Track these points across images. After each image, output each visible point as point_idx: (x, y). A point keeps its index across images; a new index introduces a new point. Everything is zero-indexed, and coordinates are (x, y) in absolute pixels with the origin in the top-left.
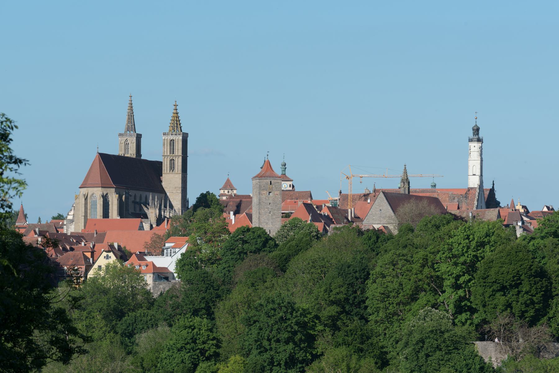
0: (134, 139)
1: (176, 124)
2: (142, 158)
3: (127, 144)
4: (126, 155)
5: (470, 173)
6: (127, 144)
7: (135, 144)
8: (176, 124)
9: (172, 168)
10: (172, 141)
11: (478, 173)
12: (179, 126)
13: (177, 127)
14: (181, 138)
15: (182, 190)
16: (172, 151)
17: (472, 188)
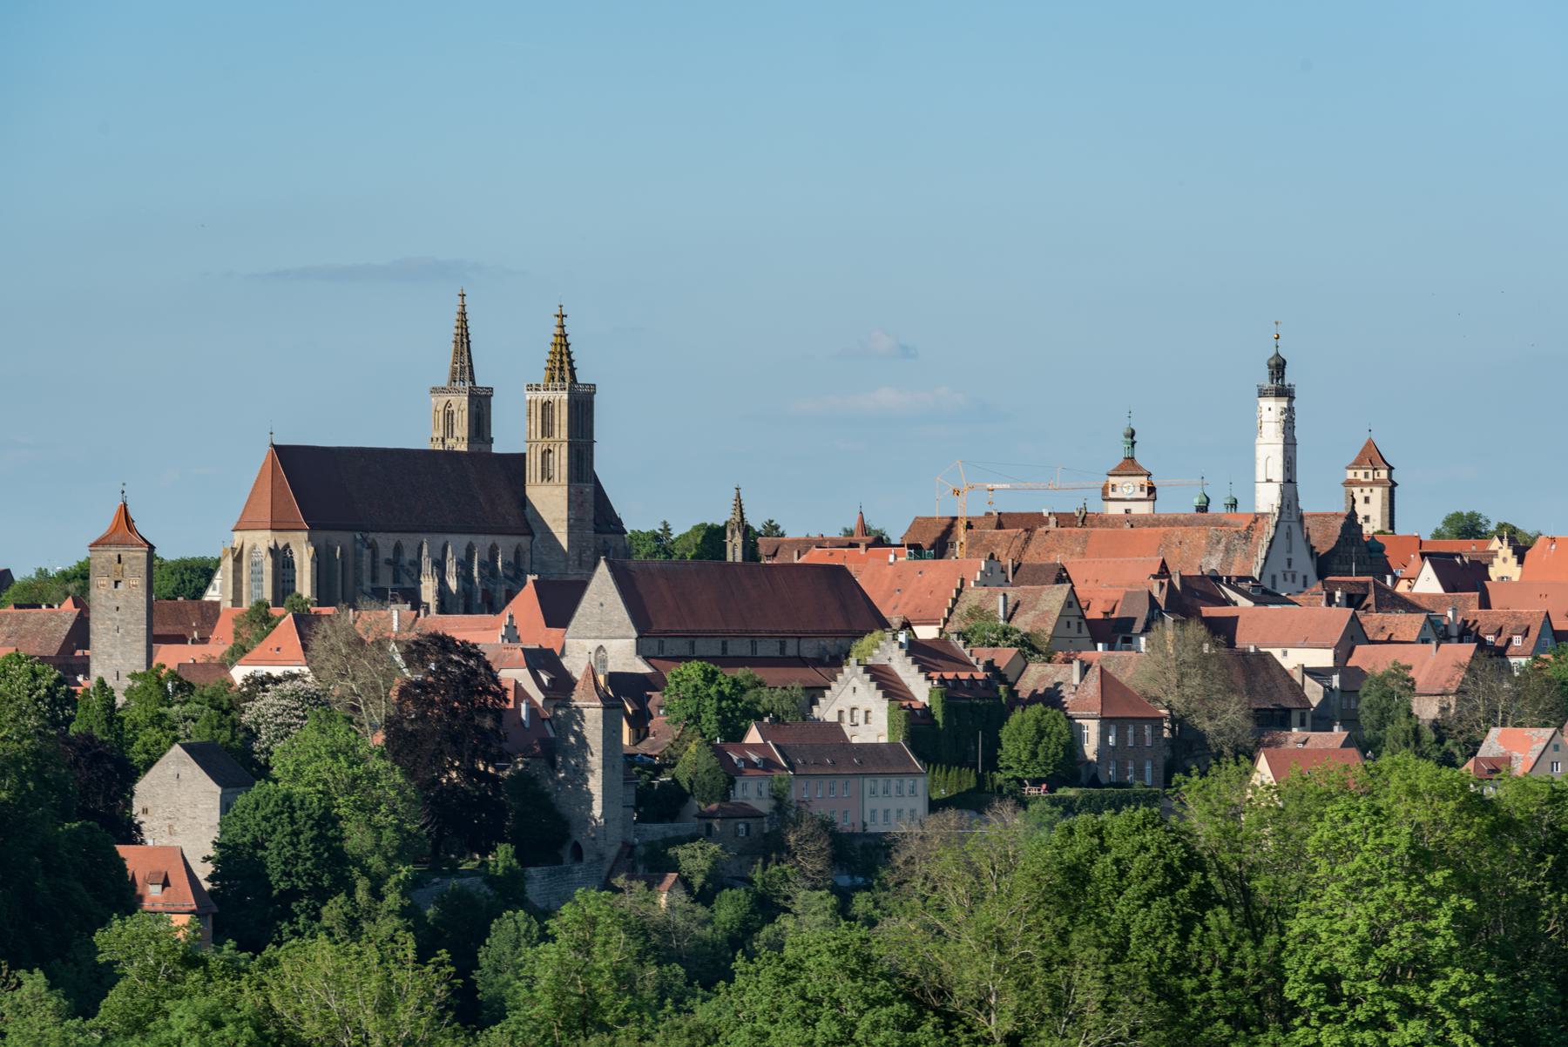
0: (463, 400)
1: (562, 362)
2: (496, 449)
3: (449, 416)
4: (450, 442)
5: (1260, 476)
6: (449, 416)
7: (466, 414)
8: (562, 362)
9: (546, 475)
10: (547, 406)
11: (1278, 474)
12: (566, 367)
13: (561, 369)
14: (565, 397)
15: (569, 526)
16: (547, 430)
17: (1264, 515)
